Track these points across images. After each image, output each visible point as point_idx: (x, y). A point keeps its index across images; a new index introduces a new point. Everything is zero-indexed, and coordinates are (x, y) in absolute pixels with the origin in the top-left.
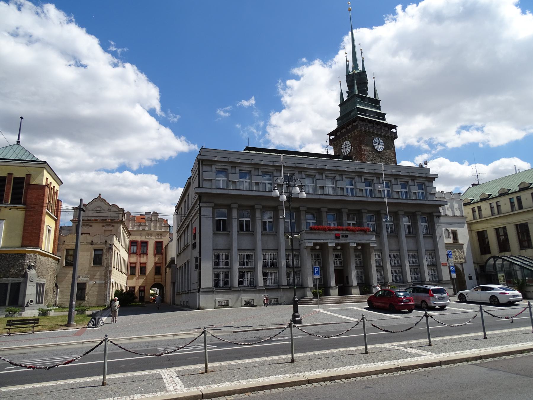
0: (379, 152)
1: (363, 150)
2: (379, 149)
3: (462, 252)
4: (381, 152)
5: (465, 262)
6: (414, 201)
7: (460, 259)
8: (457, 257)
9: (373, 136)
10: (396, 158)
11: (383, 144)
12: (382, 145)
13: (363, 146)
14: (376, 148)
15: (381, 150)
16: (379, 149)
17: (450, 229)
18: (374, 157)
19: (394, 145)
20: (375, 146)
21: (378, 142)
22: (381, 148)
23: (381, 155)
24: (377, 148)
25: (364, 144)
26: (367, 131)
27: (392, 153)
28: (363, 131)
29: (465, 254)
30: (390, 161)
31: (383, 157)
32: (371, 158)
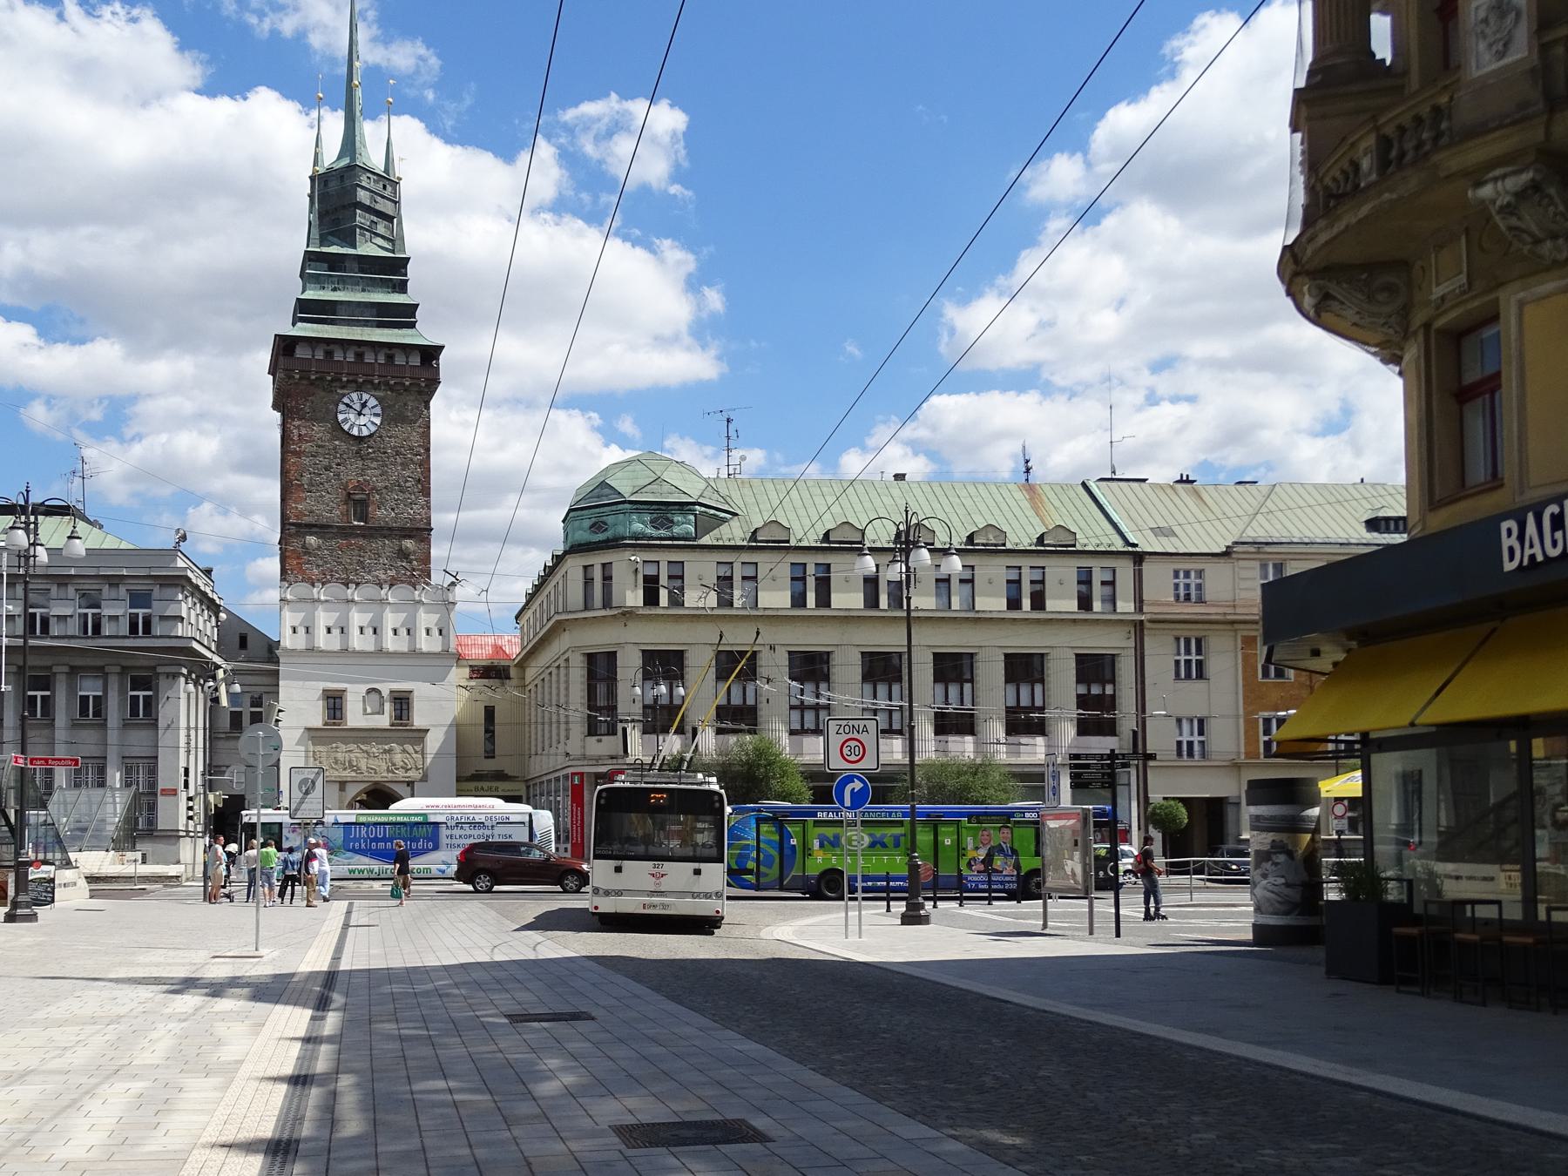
0: (360, 439)
1: (296, 438)
2: (360, 430)
3: (416, 752)
4: (371, 435)
5: (424, 779)
6: (121, 640)
7: (407, 770)
8: (394, 765)
9: (343, 387)
10: (428, 450)
11: (378, 410)
12: (376, 415)
13: (298, 427)
14: (346, 427)
15: (365, 432)
16: (360, 430)
17: (385, 689)
18: (336, 458)
19: (428, 408)
20: (346, 420)
21: (357, 407)
22: (369, 425)
23: (369, 447)
24: (352, 426)
25: (300, 419)
26: (313, 377)
27: (415, 439)
28: (301, 378)
29: (429, 761)
30: (402, 464)
31: (374, 452)
32: (326, 462)
